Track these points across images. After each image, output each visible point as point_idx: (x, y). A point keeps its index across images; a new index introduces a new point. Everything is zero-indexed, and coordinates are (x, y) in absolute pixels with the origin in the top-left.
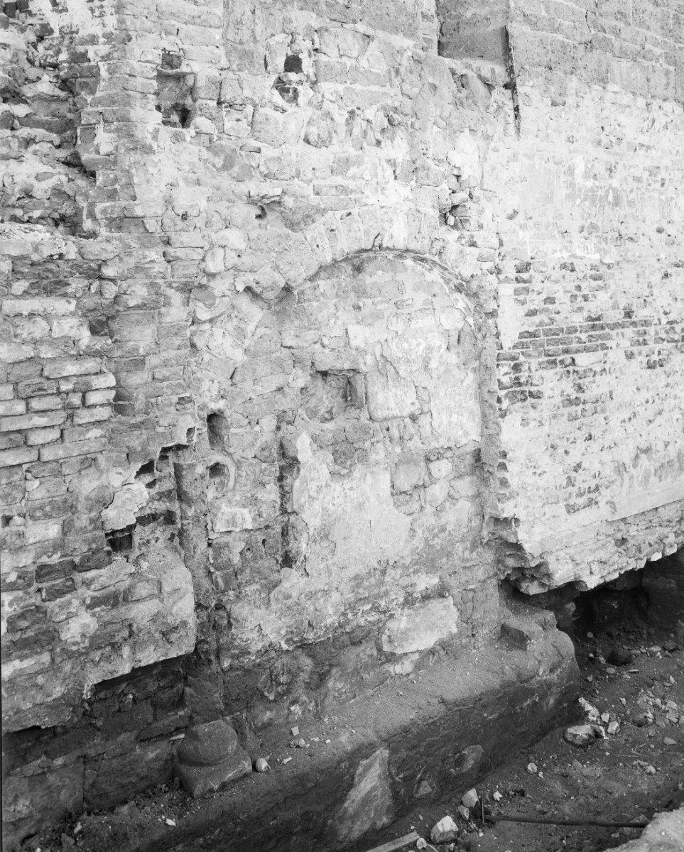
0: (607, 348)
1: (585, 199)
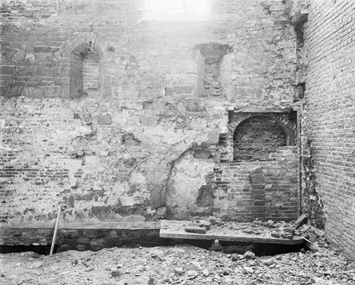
0: (15, 177)
1: (5, 132)
